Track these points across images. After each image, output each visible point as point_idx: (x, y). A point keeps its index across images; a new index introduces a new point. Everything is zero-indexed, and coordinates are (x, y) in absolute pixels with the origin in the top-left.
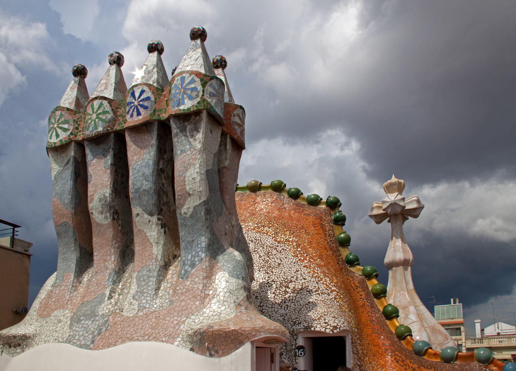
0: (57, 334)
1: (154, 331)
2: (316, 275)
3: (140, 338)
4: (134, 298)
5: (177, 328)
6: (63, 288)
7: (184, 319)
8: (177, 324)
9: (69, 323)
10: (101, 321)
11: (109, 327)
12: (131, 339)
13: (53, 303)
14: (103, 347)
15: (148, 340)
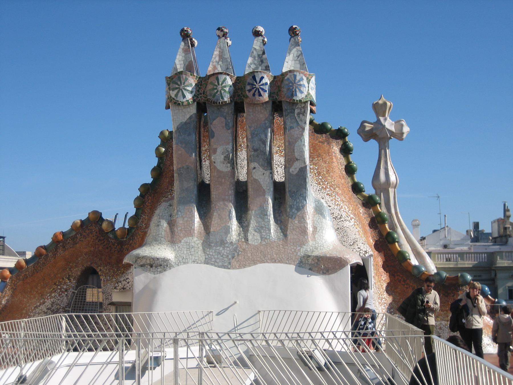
0: (193, 257)
1: (278, 256)
2: (337, 203)
3: (269, 261)
4: (255, 231)
5: (295, 254)
6: (186, 219)
7: (299, 248)
8: (295, 251)
9: (201, 248)
10: (231, 248)
11: (240, 253)
12: (262, 262)
13: (179, 232)
14: (240, 267)
15: (275, 262)
